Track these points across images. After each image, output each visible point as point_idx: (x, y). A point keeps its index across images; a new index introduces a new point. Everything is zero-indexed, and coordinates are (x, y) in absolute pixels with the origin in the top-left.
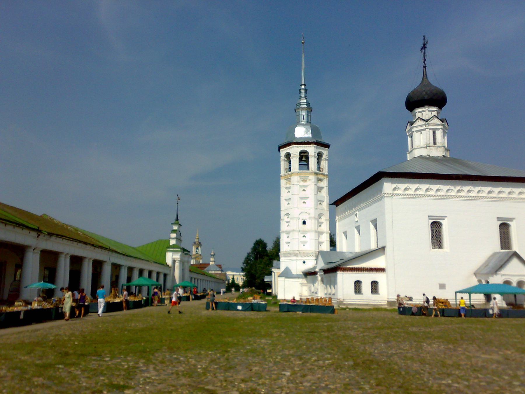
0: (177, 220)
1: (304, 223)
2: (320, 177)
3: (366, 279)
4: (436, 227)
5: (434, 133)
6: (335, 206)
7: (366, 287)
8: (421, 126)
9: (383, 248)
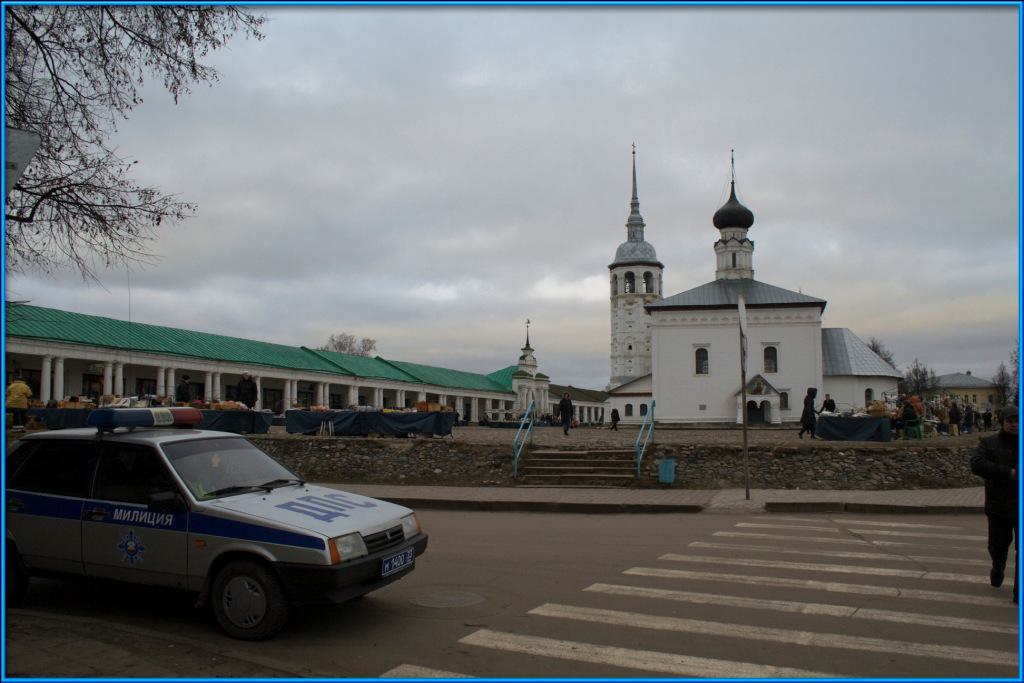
0: (528, 344)
1: (630, 347)
3: (636, 403)
4: (702, 355)
7: (636, 410)
8: (722, 248)
9: (650, 375)
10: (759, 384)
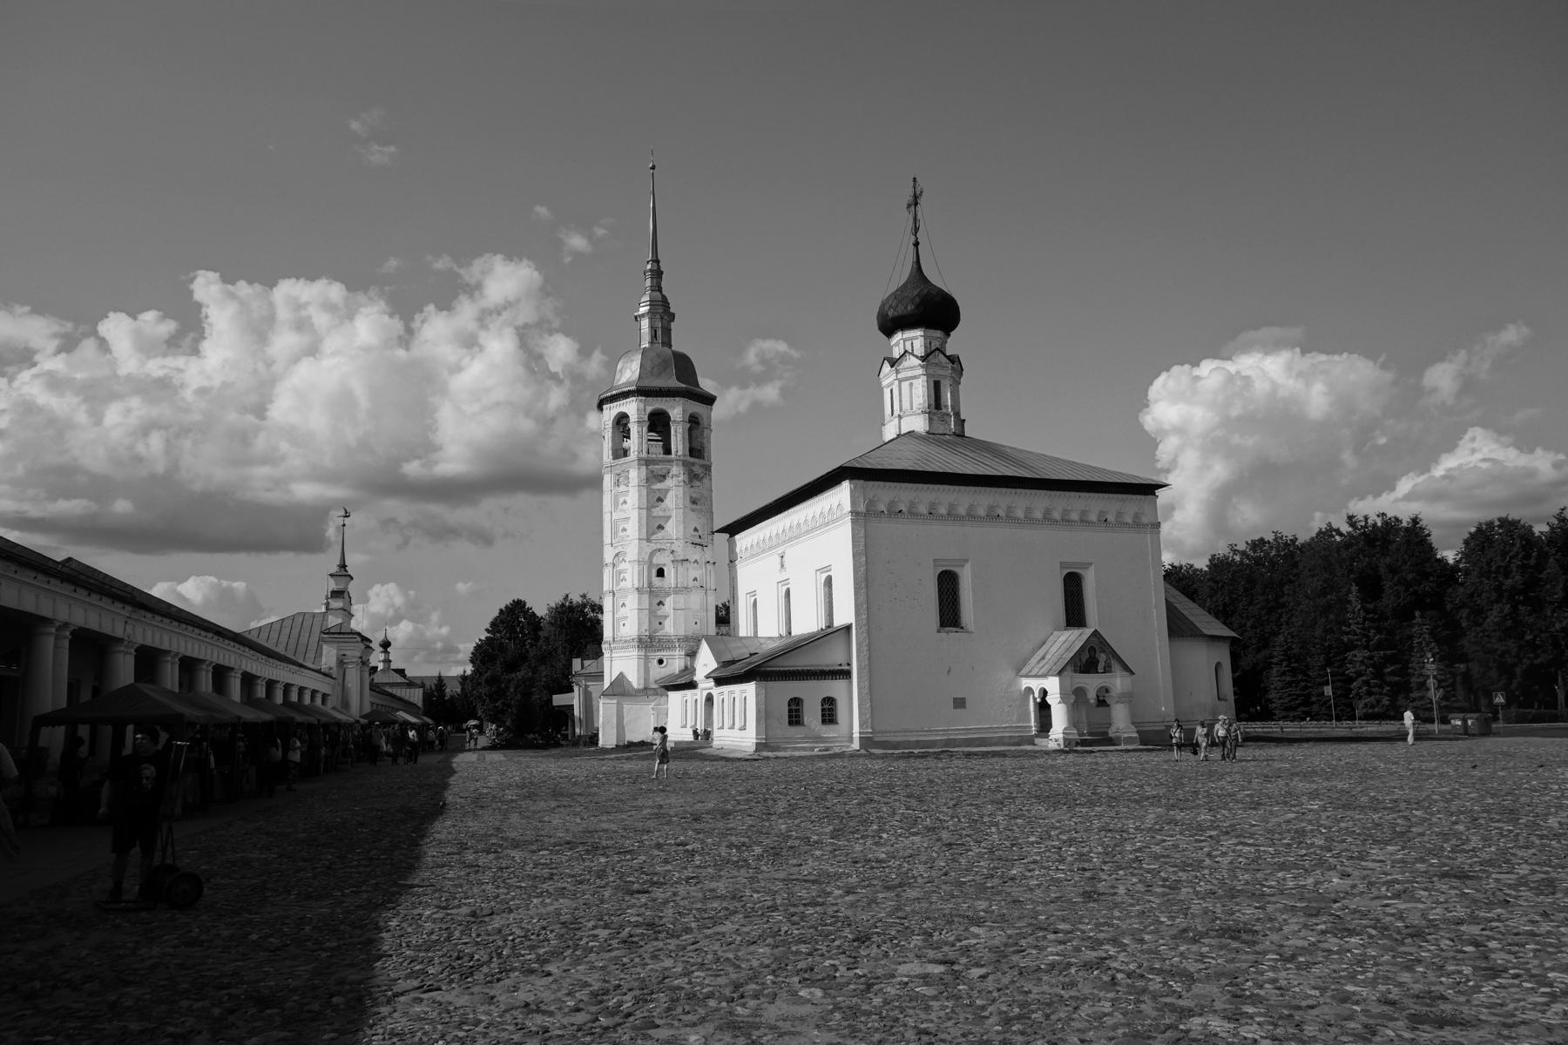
1: (661, 573)
2: (697, 469)
3: (812, 693)
4: (948, 584)
5: (937, 385)
6: (727, 536)
7: (812, 714)
8: (912, 368)
10: (1092, 649)
